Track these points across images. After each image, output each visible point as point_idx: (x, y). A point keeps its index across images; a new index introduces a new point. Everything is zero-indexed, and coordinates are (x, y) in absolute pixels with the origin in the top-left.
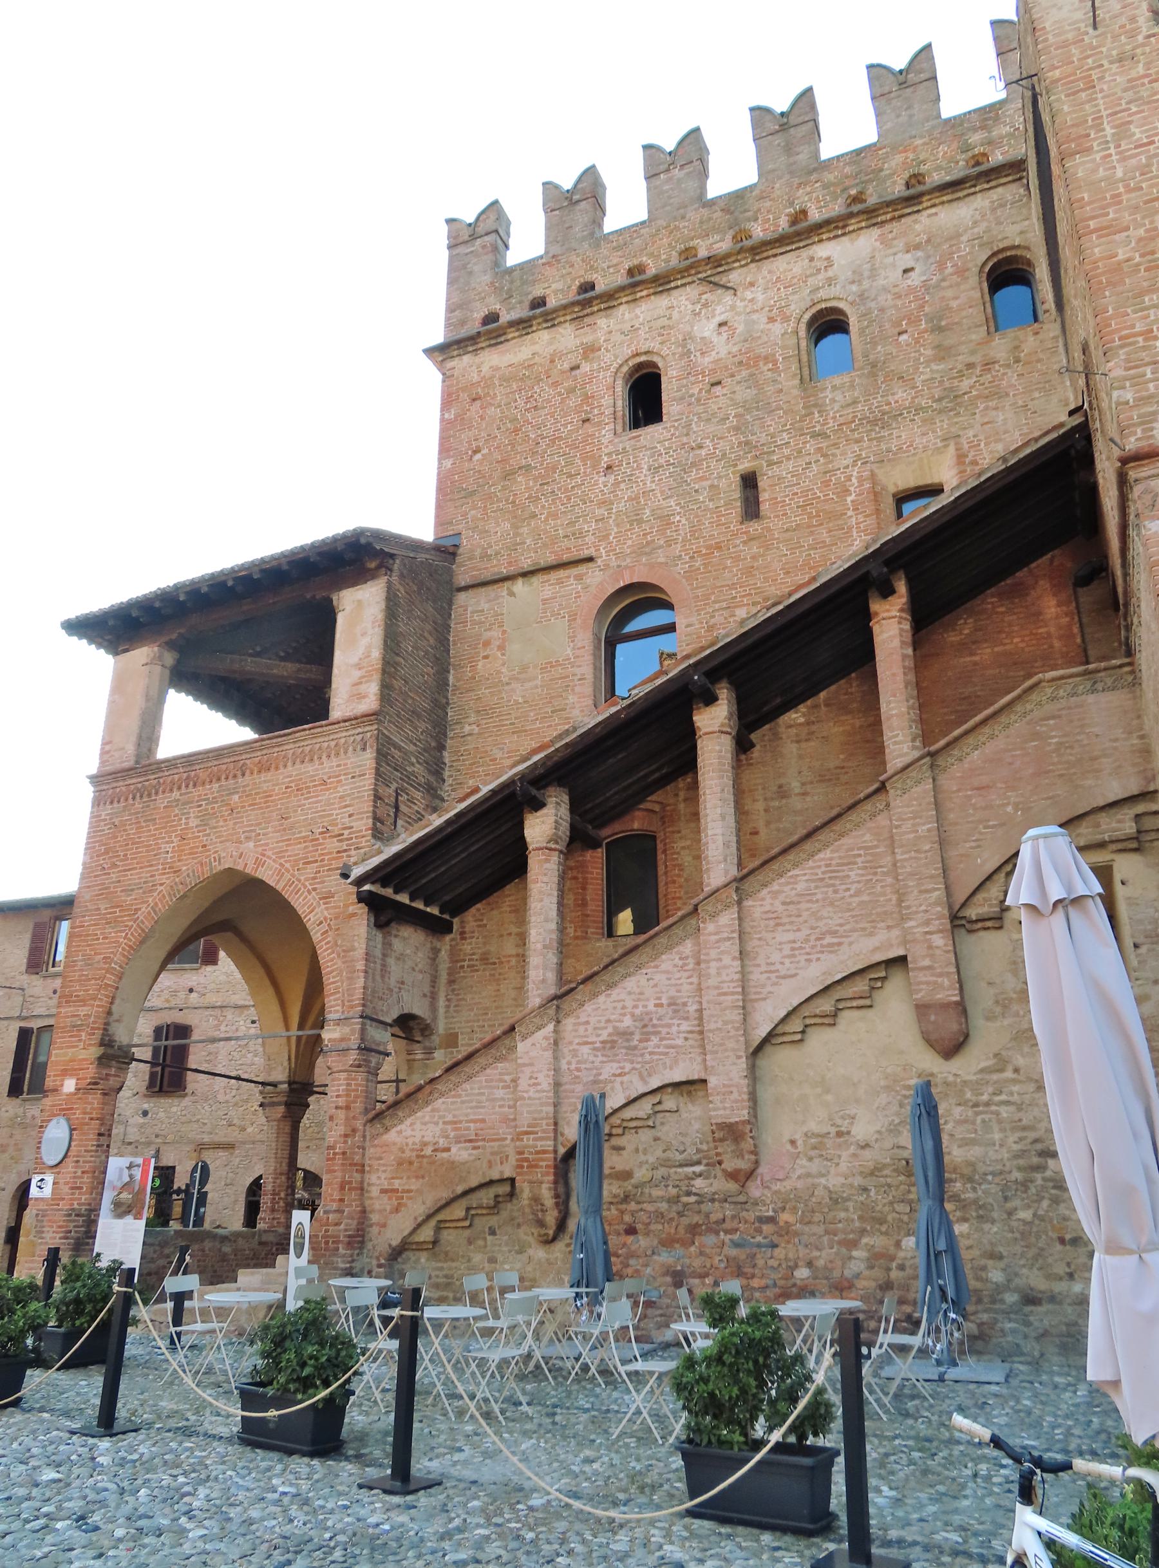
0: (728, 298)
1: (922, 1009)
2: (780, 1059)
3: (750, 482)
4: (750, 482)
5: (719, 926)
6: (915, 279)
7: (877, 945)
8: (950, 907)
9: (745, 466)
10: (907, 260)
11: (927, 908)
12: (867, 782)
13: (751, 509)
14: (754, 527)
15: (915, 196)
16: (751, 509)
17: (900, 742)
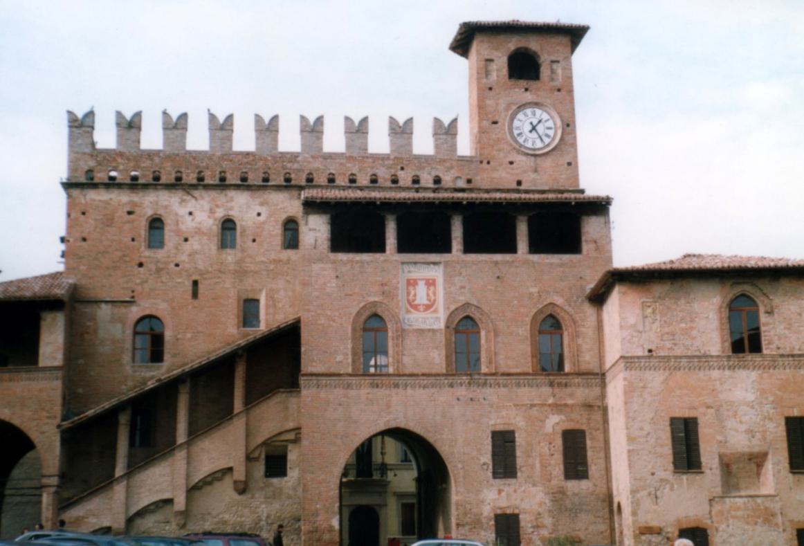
0: (193, 201)
1: (235, 482)
2: (197, 494)
3: (195, 283)
4: (195, 283)
5: (180, 456)
6: (262, 218)
7: (224, 464)
8: (247, 449)
9: (195, 277)
10: (259, 209)
11: (241, 454)
12: (226, 414)
13: (195, 295)
14: (196, 303)
15: (265, 184)
16: (195, 295)
17: (238, 404)
